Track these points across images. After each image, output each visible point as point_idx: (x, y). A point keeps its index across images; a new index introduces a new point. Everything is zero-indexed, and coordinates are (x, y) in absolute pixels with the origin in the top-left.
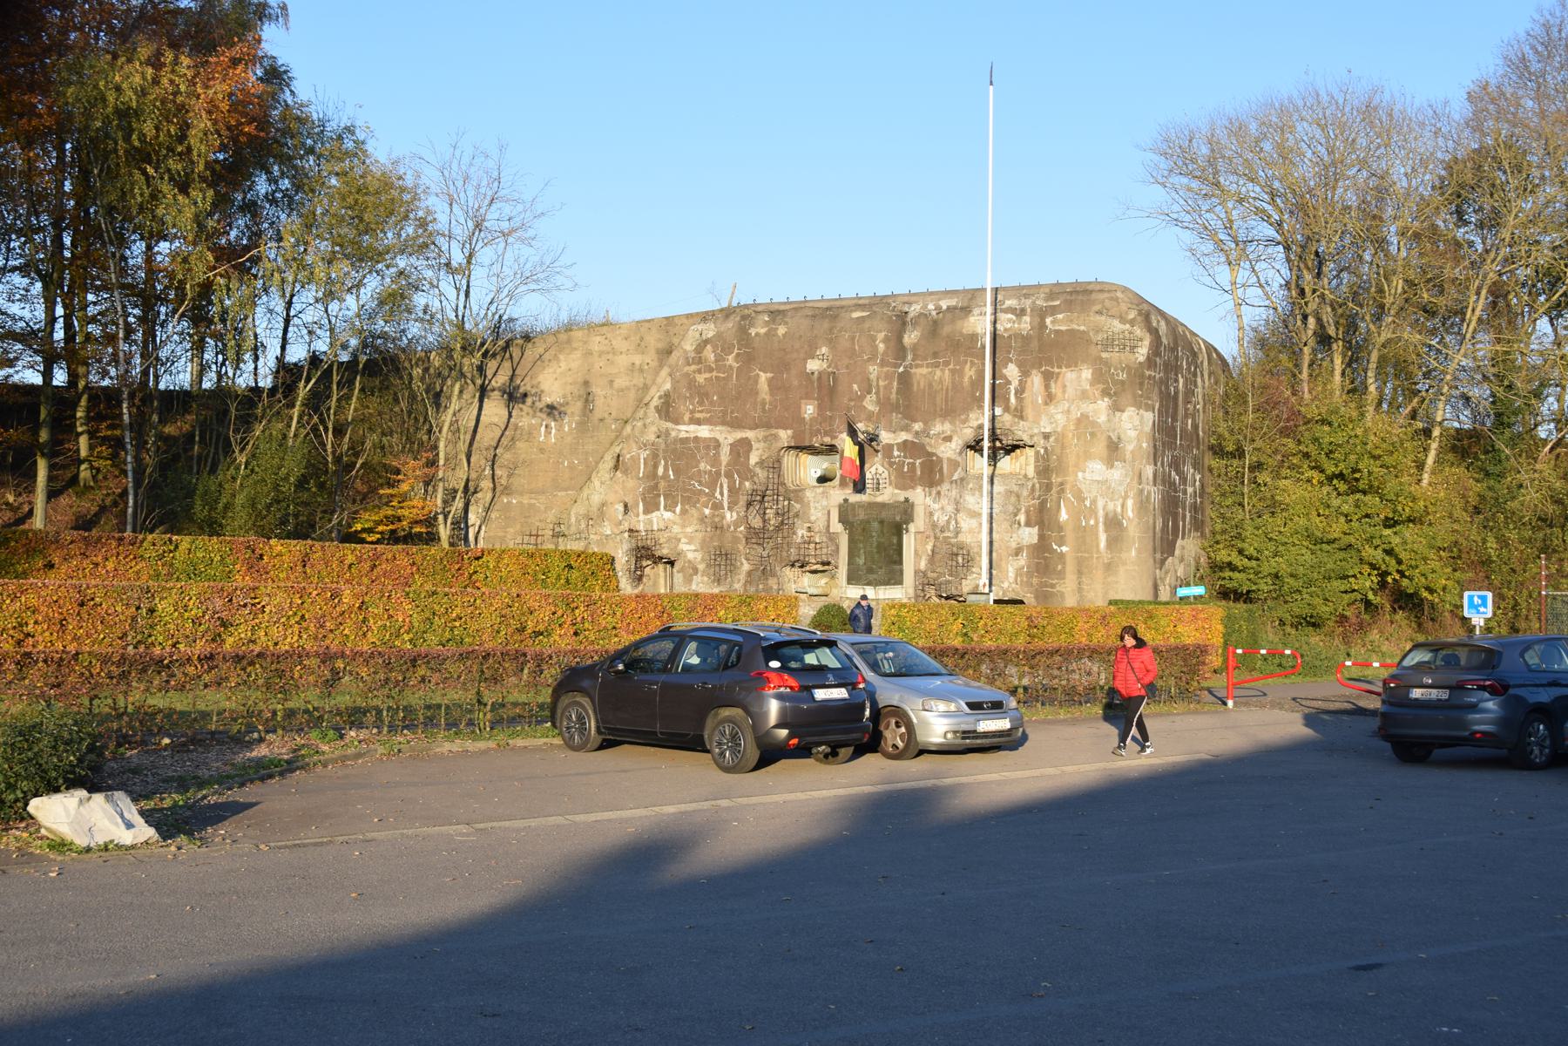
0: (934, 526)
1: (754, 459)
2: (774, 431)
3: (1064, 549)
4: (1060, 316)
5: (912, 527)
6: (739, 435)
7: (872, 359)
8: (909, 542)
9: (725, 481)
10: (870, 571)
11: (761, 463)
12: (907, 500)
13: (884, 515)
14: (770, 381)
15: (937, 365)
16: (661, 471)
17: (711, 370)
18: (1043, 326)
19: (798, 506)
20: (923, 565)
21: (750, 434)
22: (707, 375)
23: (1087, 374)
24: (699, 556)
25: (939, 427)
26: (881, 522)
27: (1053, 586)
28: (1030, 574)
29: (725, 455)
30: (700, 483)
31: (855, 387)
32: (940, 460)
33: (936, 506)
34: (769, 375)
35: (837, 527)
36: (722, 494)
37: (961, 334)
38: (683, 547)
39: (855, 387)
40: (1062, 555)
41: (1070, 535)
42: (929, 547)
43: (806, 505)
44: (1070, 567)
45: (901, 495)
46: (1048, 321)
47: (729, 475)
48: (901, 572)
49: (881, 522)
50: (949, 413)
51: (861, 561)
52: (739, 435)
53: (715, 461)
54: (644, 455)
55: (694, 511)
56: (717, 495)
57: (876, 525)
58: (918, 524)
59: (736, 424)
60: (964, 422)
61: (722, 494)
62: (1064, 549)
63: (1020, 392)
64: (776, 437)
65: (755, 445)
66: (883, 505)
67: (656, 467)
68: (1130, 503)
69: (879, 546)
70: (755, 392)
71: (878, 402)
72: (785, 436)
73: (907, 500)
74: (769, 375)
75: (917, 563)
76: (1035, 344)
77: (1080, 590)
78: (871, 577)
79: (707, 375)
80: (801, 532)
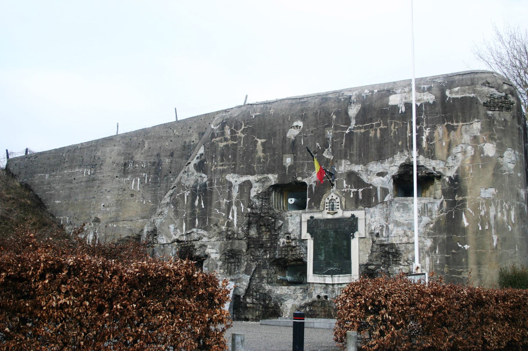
1: (253, 194)
2: (266, 175)
3: (466, 247)
4: (456, 89)
5: (356, 235)
6: (244, 179)
7: (329, 126)
8: (355, 243)
9: (234, 208)
10: (329, 265)
11: (257, 196)
12: (353, 216)
14: (263, 144)
15: (372, 126)
16: (197, 202)
17: (226, 140)
18: (444, 96)
19: (281, 222)
21: (251, 178)
22: (225, 143)
23: (477, 126)
24: (218, 256)
25: (375, 167)
27: (460, 273)
28: (442, 265)
29: (235, 193)
30: (220, 209)
31: (318, 144)
32: (375, 189)
34: (263, 140)
35: (306, 235)
36: (233, 217)
37: (387, 105)
38: (208, 250)
39: (318, 144)
40: (466, 252)
41: (470, 236)
43: (286, 222)
44: (472, 258)
46: (447, 93)
47: (238, 204)
49: (336, 232)
50: (381, 158)
51: (322, 258)
52: (244, 179)
53: (230, 197)
54: (187, 193)
55: (216, 228)
56: (230, 217)
57: (332, 233)
58: (362, 230)
59: (242, 173)
60: (391, 162)
61: (233, 217)
62: (466, 247)
63: (430, 139)
64: (267, 179)
65: (255, 184)
67: (193, 201)
68: (513, 213)
69: (335, 248)
70: (254, 151)
71: (333, 153)
72: (273, 179)
73: (353, 216)
74: (263, 140)
76: (438, 108)
77: (479, 276)
79: (225, 143)
80: (282, 241)
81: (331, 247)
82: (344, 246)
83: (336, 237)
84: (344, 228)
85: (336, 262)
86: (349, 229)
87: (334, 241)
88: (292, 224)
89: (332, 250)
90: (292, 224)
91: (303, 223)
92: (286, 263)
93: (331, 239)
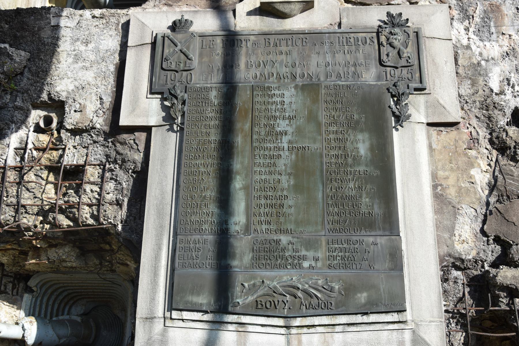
0: (488, 106)
5: (418, 109)
8: (413, 151)
12: (394, 21)
13: (316, 64)
19: (20, 56)
20: (467, 240)
26: (310, 88)
33: (494, 49)
35: (142, 108)
42: (481, 177)
45: (373, 16)
48: (395, 260)
49: (310, 88)
57: (289, 96)
58: (444, 91)
66: (312, 37)
69: (301, 170)
73: (394, 21)
75: (445, 228)
78: (278, 278)
81: (281, 164)
82: (357, 160)
83: (312, 117)
84: (356, 75)
85: (310, 245)
86: (379, 78)
87: (299, 131)
88: (77, 58)
89: (285, 182)
90: (77, 58)
91: (130, 55)
92: (24, 254)
93: (282, 125)
